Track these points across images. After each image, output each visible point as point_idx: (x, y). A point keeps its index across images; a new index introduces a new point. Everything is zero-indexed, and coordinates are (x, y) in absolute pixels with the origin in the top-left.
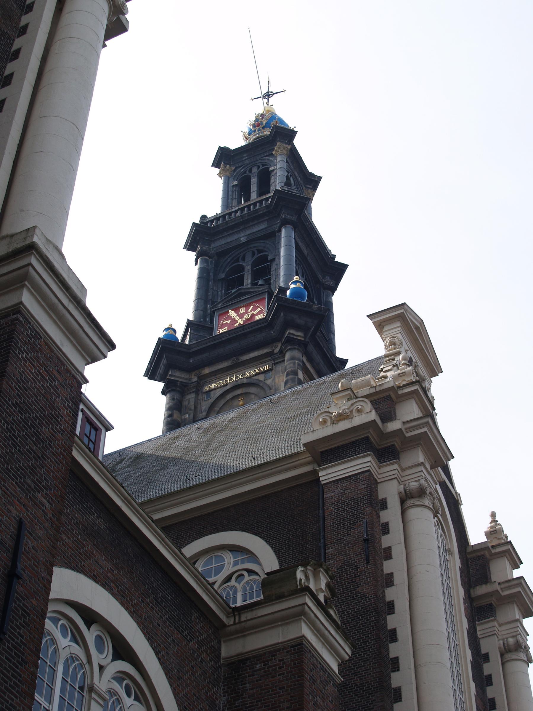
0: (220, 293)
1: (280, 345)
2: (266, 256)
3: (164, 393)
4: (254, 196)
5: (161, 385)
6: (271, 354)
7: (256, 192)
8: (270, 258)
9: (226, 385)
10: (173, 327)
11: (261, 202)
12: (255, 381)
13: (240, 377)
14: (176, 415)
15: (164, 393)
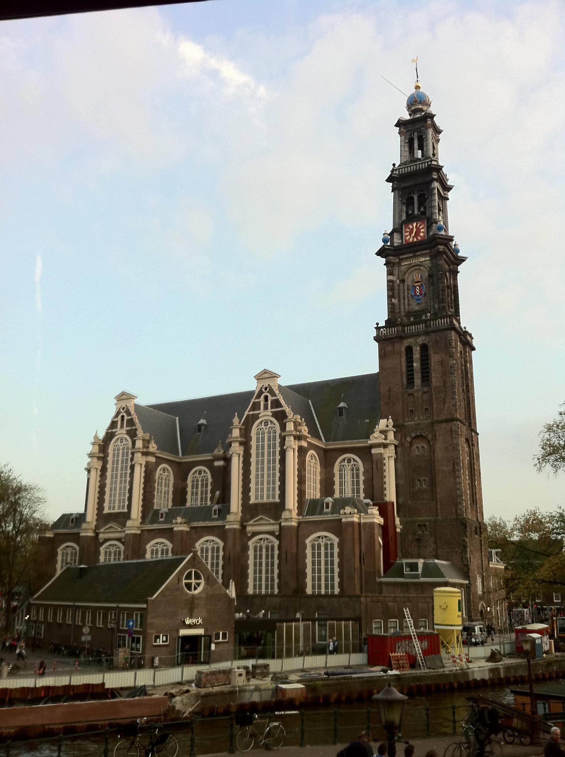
8: (426, 196)
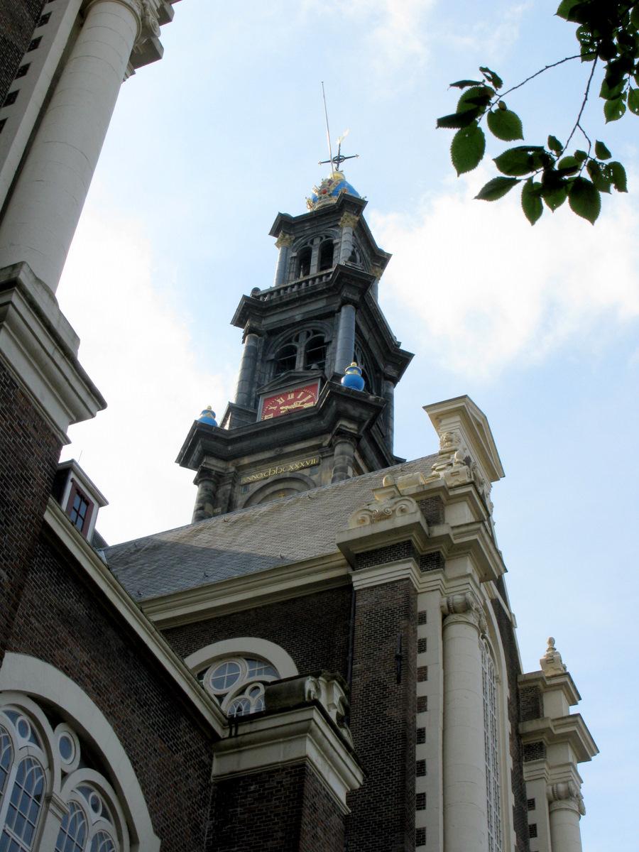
0: (267, 375)
1: (329, 437)
2: (322, 338)
3: (196, 482)
4: (314, 270)
5: (193, 474)
6: (319, 447)
7: (316, 267)
8: (326, 340)
9: (267, 478)
10: (212, 410)
11: (321, 277)
12: (299, 476)
13: (282, 470)
14: (208, 507)
15: (196, 482)
